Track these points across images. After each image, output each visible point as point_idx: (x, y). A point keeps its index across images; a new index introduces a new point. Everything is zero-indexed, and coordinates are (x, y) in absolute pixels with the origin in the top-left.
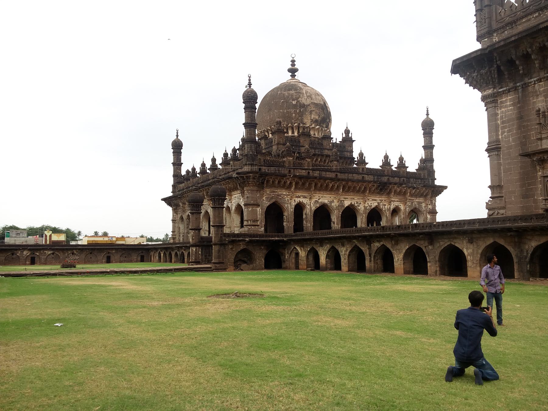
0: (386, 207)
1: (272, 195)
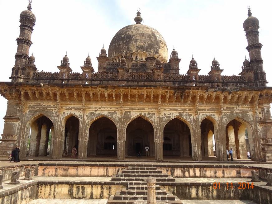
0: (192, 117)
1: (37, 108)
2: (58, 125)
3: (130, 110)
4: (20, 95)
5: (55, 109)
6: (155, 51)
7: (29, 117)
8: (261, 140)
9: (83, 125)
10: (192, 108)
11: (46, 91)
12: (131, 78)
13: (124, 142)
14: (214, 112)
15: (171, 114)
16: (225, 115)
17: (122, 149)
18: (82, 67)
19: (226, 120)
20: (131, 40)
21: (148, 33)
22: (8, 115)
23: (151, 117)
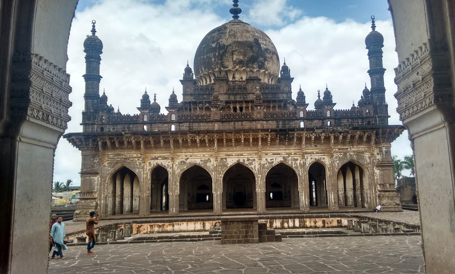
0: (298, 162)
1: (117, 159)
2: (143, 178)
3: (226, 157)
4: (98, 145)
5: (139, 160)
6: (259, 65)
7: (109, 171)
8: (378, 186)
9: (172, 177)
10: (298, 151)
11: (127, 140)
12: (226, 117)
13: (220, 194)
14: (324, 155)
15: (274, 160)
16: (336, 157)
17: (219, 202)
18: (166, 108)
19: (338, 164)
20: (226, 51)
21: (248, 40)
22: (85, 170)
23: (251, 164)
